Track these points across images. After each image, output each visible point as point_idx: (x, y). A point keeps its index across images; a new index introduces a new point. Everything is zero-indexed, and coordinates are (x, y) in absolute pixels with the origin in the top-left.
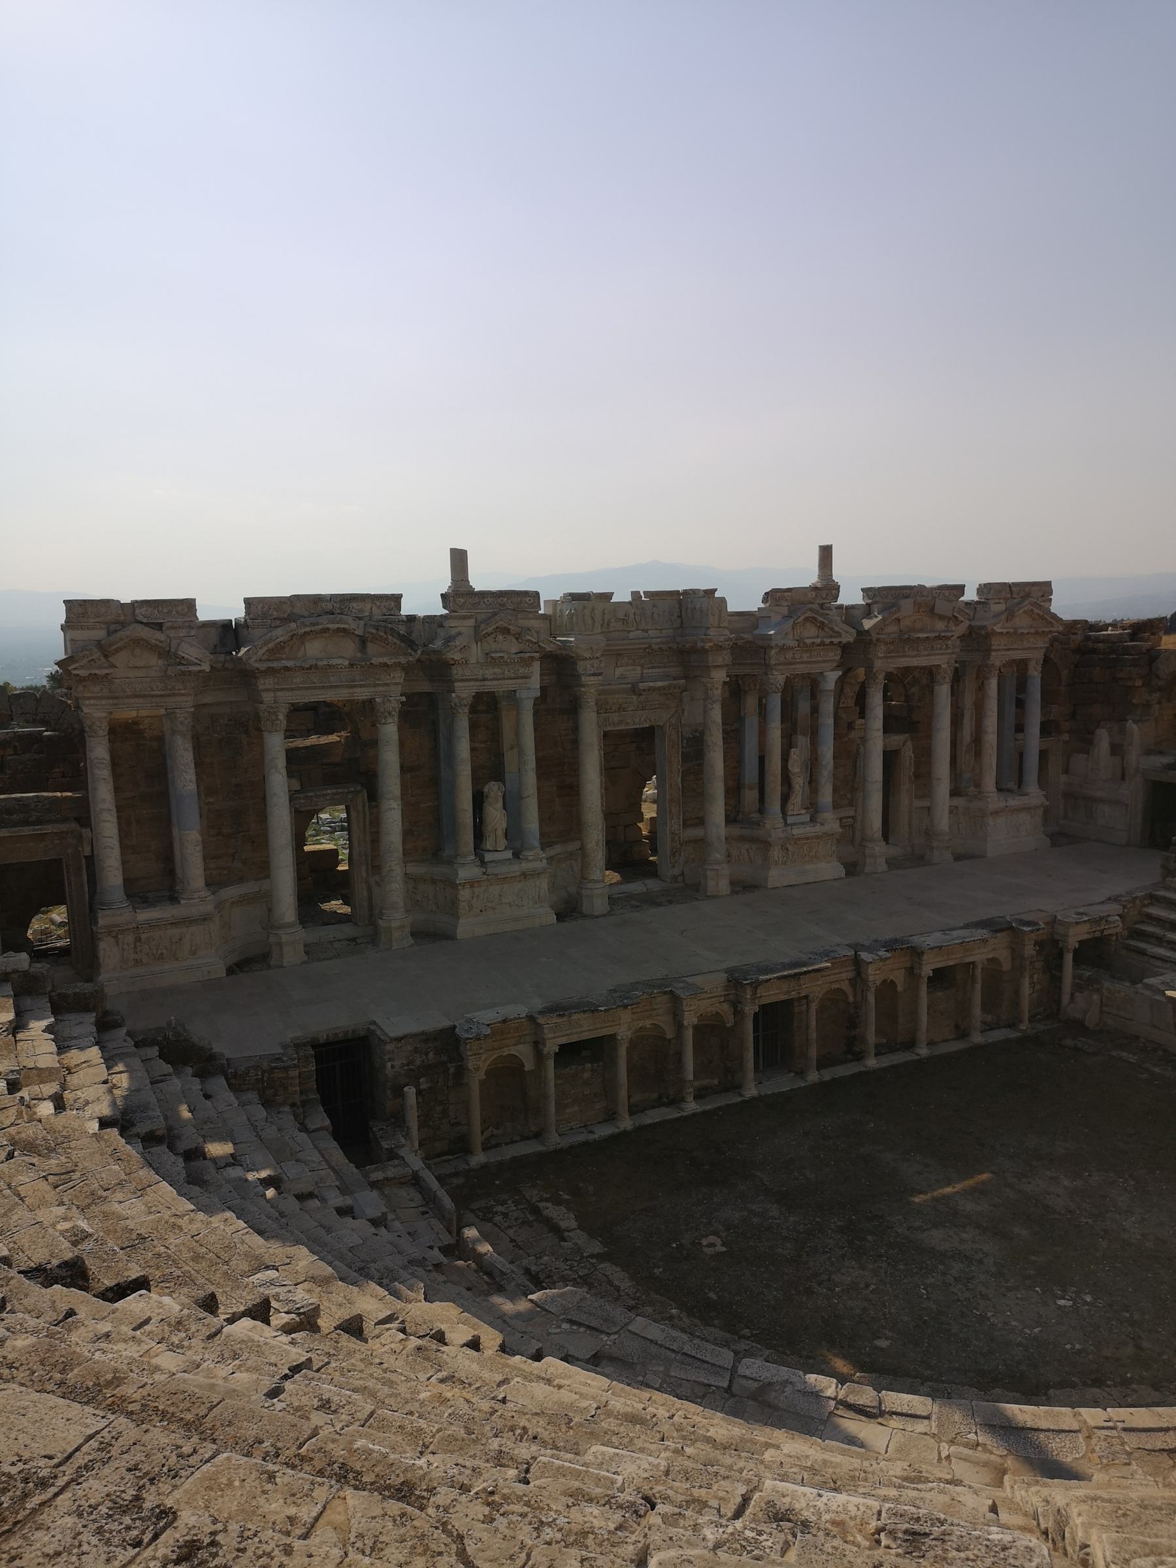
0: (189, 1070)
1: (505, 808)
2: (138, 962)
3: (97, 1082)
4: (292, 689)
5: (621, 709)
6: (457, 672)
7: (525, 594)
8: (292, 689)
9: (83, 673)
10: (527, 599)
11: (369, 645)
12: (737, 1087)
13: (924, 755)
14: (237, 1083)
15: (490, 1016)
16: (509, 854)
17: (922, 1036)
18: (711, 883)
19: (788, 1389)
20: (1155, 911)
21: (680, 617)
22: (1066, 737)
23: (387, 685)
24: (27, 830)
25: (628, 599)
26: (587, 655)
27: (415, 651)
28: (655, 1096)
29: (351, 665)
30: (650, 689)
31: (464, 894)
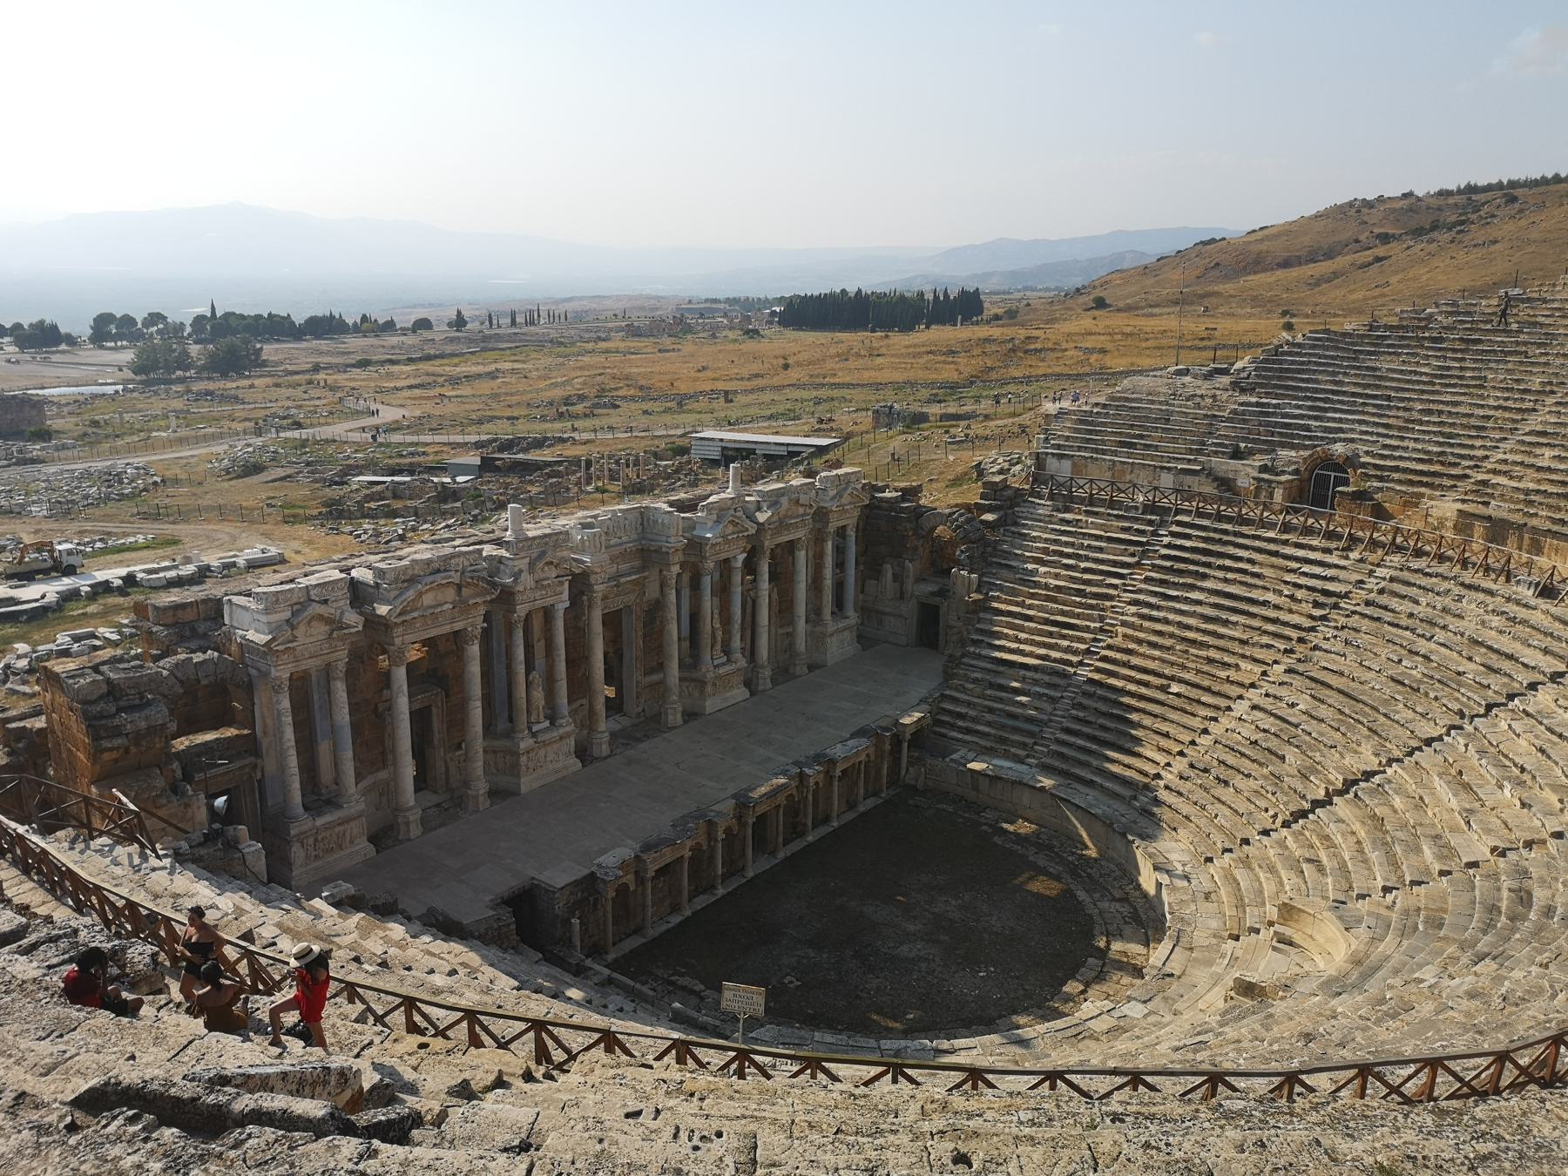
6: (519, 598)
16: (547, 723)
18: (671, 717)
31: (523, 759)
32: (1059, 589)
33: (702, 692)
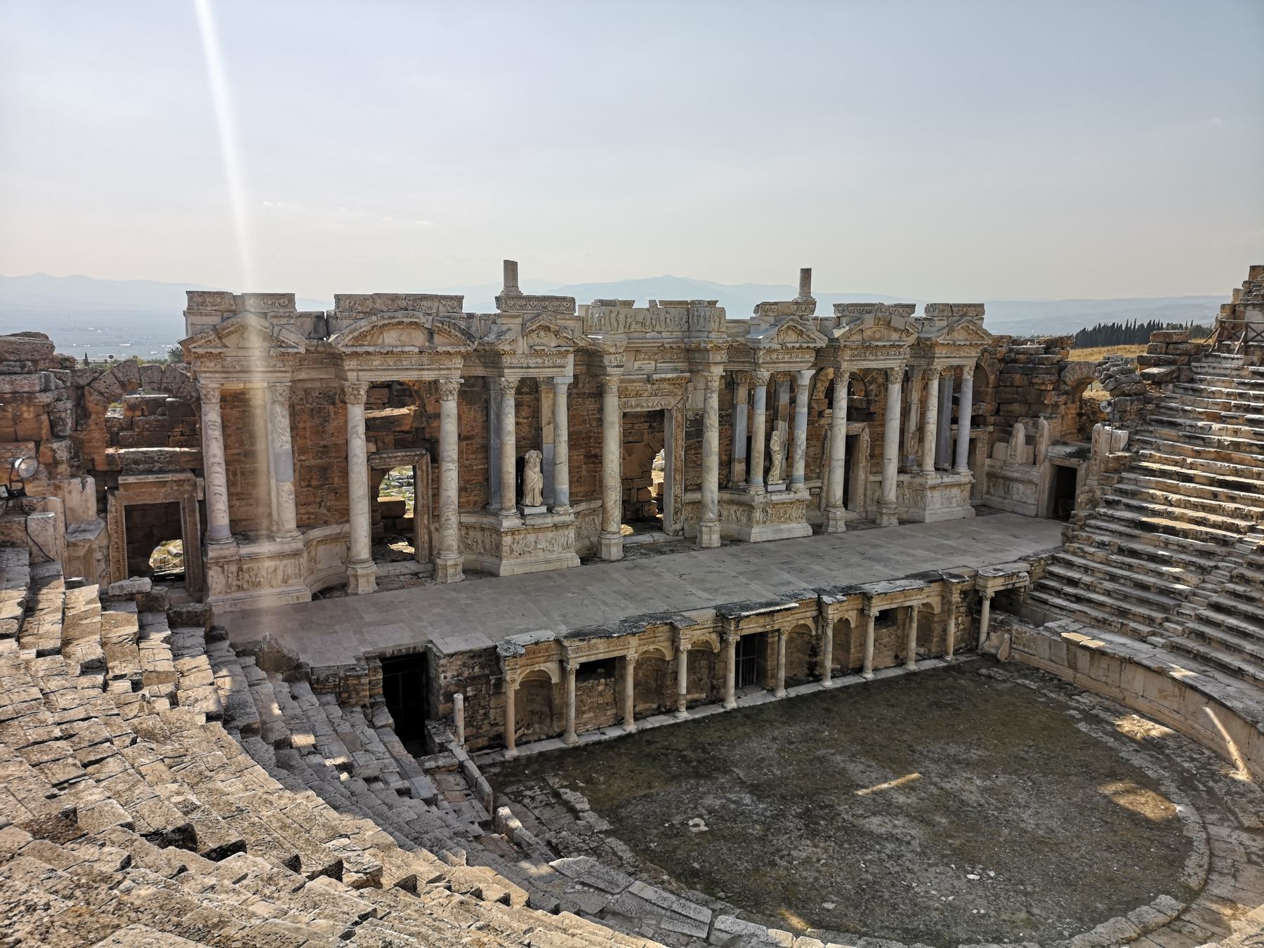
0: (280, 676)
1: (541, 471)
2: (240, 588)
3: (205, 683)
5: (638, 395)
6: (506, 360)
7: (564, 299)
9: (200, 351)
11: (436, 336)
12: (721, 701)
13: (879, 440)
14: (318, 687)
15: (525, 638)
16: (544, 509)
17: (869, 664)
18: (705, 537)
19: (754, 941)
20: (1056, 569)
22: (991, 428)
24: (151, 478)
25: (647, 306)
26: (612, 350)
28: (654, 706)
29: (421, 352)
31: (507, 540)
32: (1236, 446)
33: (750, 519)
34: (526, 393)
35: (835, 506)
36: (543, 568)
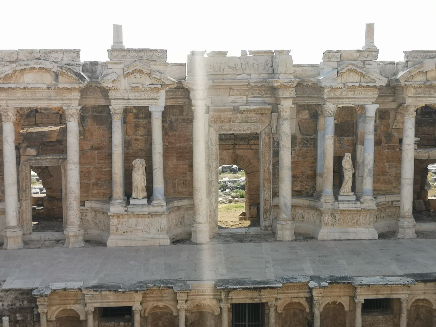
4: (16, 100)
6: (111, 94)
8: (16, 100)
10: (157, 54)
11: (60, 77)
16: (145, 201)
18: (279, 233)
21: (272, 66)
23: (69, 99)
27: (84, 81)
29: (48, 88)
30: (248, 110)
31: (114, 221)
34: (142, 118)
35: (404, 217)
36: (140, 243)
